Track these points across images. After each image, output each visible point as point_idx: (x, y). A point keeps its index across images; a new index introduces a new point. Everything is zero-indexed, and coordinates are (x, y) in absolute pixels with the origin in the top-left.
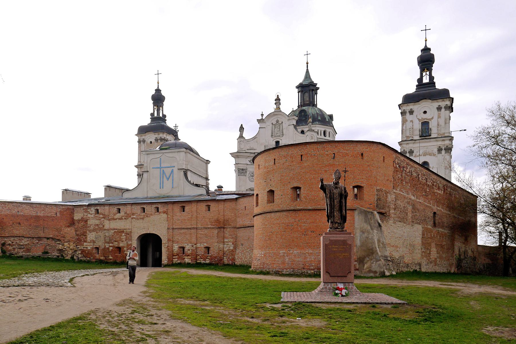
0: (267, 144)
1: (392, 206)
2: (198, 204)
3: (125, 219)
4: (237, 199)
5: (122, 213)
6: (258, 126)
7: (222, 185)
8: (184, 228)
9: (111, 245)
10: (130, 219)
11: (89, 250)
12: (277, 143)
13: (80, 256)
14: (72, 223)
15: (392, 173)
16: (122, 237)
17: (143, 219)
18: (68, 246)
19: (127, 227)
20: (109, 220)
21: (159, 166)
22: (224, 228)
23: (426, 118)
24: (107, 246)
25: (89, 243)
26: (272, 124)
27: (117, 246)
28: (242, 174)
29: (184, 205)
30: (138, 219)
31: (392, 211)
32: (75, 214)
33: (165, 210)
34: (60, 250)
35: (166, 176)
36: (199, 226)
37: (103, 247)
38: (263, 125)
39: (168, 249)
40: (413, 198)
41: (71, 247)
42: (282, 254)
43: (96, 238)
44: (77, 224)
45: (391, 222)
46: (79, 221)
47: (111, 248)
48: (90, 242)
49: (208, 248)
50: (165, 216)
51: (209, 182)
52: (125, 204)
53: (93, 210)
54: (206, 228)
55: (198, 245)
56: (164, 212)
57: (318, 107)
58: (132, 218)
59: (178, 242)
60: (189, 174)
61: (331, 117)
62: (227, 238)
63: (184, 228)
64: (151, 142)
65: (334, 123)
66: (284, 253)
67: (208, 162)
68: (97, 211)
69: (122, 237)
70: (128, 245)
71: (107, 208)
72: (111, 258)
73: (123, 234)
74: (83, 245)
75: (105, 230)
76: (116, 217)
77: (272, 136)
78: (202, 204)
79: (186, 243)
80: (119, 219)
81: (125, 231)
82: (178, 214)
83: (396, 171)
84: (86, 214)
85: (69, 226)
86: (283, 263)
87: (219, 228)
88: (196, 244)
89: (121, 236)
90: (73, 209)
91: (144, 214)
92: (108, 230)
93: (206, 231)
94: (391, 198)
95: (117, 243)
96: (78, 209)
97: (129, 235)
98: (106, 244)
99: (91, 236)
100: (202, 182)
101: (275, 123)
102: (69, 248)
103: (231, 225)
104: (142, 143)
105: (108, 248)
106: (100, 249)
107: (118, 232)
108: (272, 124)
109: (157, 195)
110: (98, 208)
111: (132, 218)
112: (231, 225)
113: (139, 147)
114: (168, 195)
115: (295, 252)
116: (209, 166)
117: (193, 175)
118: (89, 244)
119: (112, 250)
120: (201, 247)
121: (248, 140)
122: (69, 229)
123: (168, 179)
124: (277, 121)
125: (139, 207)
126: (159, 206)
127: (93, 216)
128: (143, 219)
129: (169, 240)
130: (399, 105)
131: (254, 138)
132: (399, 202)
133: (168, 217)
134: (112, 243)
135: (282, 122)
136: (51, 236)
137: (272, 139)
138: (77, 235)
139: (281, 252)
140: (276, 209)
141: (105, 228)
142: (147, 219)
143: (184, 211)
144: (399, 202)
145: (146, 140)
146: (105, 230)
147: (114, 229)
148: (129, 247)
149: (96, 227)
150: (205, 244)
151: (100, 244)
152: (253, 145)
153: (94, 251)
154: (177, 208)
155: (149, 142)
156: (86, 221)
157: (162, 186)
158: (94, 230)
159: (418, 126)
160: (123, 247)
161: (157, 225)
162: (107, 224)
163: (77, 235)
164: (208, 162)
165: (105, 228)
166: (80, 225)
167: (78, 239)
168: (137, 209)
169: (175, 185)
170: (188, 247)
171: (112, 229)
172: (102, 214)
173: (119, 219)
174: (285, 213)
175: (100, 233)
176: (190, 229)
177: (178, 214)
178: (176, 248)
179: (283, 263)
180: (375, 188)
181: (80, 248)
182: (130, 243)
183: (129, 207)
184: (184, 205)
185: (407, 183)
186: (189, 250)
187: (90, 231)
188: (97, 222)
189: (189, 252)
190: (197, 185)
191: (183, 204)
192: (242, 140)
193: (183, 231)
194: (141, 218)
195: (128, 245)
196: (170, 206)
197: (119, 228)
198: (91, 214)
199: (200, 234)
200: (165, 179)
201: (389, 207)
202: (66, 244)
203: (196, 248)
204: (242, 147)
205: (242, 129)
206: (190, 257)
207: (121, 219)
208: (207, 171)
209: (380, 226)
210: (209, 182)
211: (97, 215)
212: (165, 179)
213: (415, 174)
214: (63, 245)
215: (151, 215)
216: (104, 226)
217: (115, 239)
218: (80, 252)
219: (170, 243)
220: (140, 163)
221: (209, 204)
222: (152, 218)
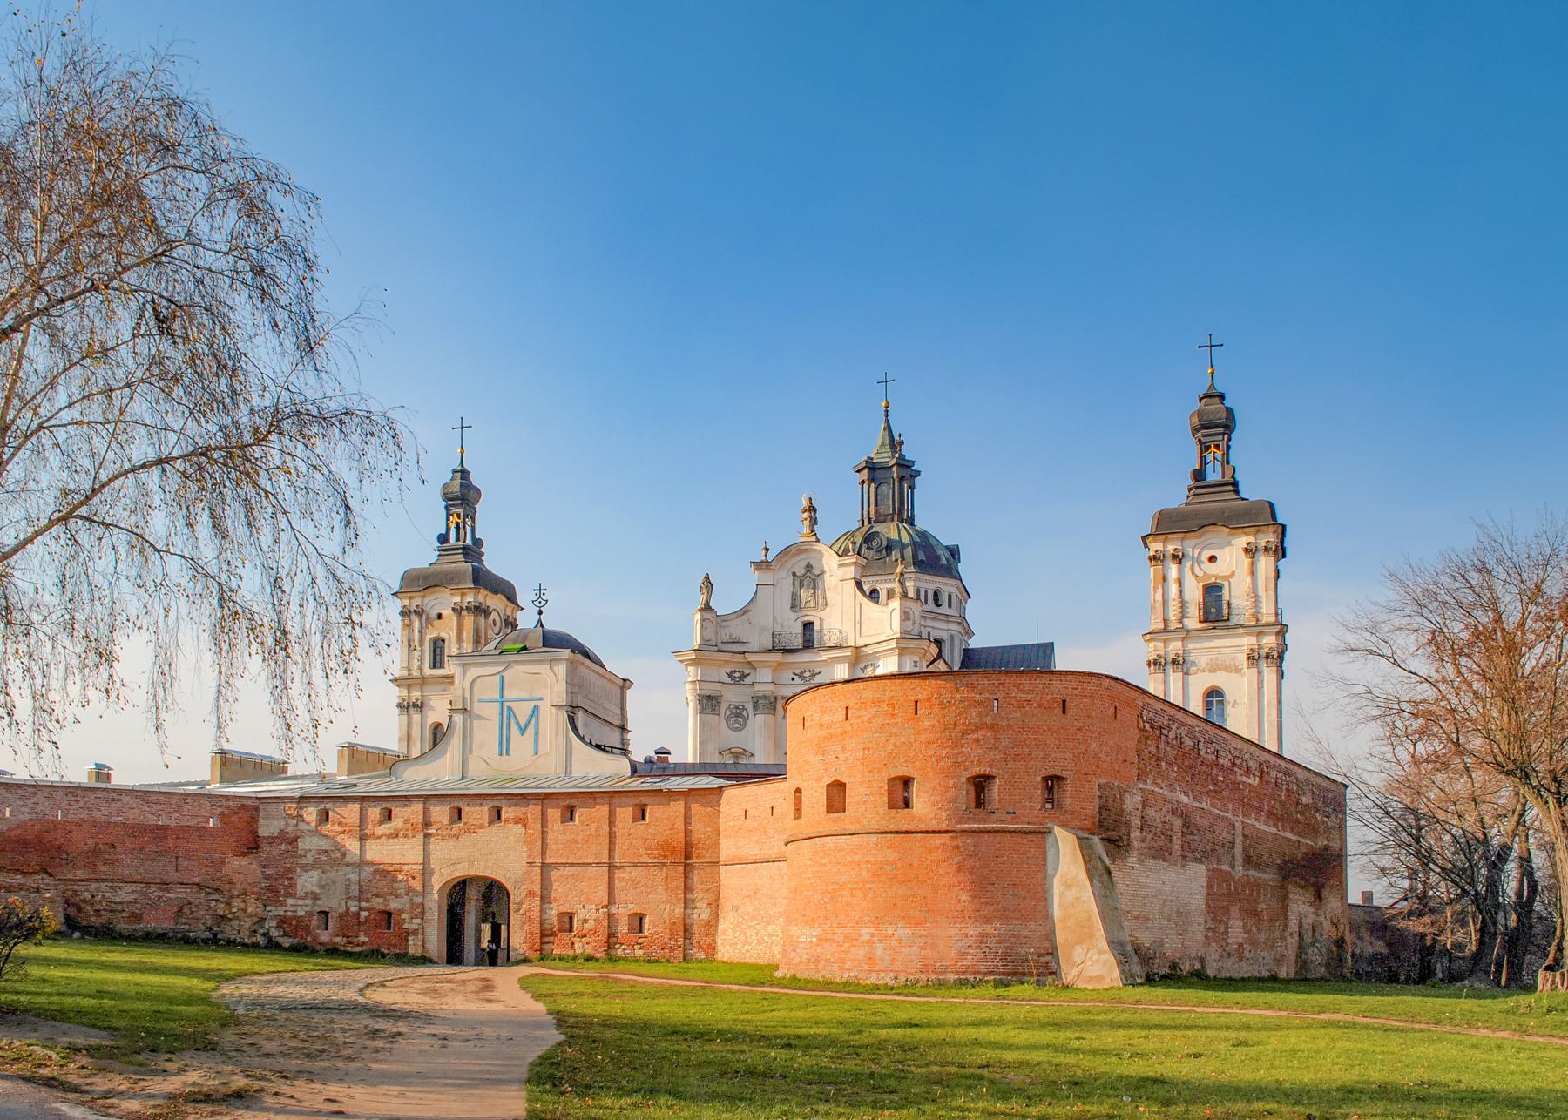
0: (778, 629)
1: (1136, 822)
2: (616, 800)
3: (406, 836)
4: (720, 789)
5: (397, 822)
6: (755, 577)
7: (669, 748)
8: (572, 864)
9: (363, 904)
11: (299, 919)
12: (808, 626)
13: (274, 933)
14: (252, 845)
15: (1133, 744)
17: (457, 837)
21: (497, 696)
24: (353, 909)
26: (794, 574)
29: (573, 802)
31: (1135, 834)
32: (261, 822)
38: (767, 577)
40: (1185, 799)
42: (866, 938)
43: (322, 887)
44: (266, 848)
45: (1133, 859)
46: (272, 840)
47: (364, 914)
50: (519, 829)
51: (629, 736)
52: (407, 799)
54: (635, 865)
55: (614, 910)
56: (517, 821)
57: (920, 524)
60: (581, 717)
61: (954, 552)
63: (572, 864)
65: (962, 568)
66: (872, 935)
67: (626, 683)
70: (414, 906)
74: (283, 904)
75: (348, 865)
77: (793, 607)
78: (623, 800)
80: (390, 836)
81: (405, 868)
83: (1144, 736)
85: (244, 854)
86: (871, 959)
90: (257, 809)
93: (635, 872)
94: (1132, 802)
96: (272, 808)
99: (307, 881)
100: (613, 739)
101: (800, 571)
104: (413, 616)
105: (357, 915)
106: (333, 915)
108: (794, 574)
110: (329, 806)
113: (408, 626)
114: (521, 774)
115: (901, 932)
116: (629, 693)
117: (590, 719)
118: (300, 902)
121: (725, 619)
122: (244, 861)
123: (523, 731)
124: (809, 568)
126: (502, 803)
128: (457, 837)
129: (530, 894)
130: (1144, 538)
131: (744, 611)
132: (1151, 812)
135: (823, 573)
136: (196, 880)
137: (792, 615)
138: (267, 878)
139: (864, 931)
140: (853, 828)
142: (464, 838)
143: (571, 819)
144: (1151, 812)
146: (348, 865)
149: (323, 858)
151: (335, 903)
152: (737, 629)
156: (295, 839)
157: (505, 747)
158: (313, 867)
159: (1194, 593)
160: (400, 912)
161: (499, 852)
163: (267, 878)
164: (626, 683)
166: (275, 852)
167: (270, 889)
168: (440, 813)
173: (390, 836)
174: (873, 838)
175: (332, 874)
179: (871, 959)
180: (1096, 781)
183: (418, 807)
184: (573, 802)
185: (1170, 764)
187: (306, 868)
188: (325, 844)
190: (598, 747)
191: (570, 804)
192: (708, 615)
193: (569, 871)
195: (414, 906)
200: (515, 730)
201: (1128, 825)
204: (710, 634)
205: (708, 585)
208: (623, 708)
209: (1109, 873)
210: (629, 736)
212: (515, 730)
213: (1188, 742)
214: (228, 904)
215: (481, 826)
216: (344, 855)
218: (274, 924)
220: (405, 673)
221: (644, 800)
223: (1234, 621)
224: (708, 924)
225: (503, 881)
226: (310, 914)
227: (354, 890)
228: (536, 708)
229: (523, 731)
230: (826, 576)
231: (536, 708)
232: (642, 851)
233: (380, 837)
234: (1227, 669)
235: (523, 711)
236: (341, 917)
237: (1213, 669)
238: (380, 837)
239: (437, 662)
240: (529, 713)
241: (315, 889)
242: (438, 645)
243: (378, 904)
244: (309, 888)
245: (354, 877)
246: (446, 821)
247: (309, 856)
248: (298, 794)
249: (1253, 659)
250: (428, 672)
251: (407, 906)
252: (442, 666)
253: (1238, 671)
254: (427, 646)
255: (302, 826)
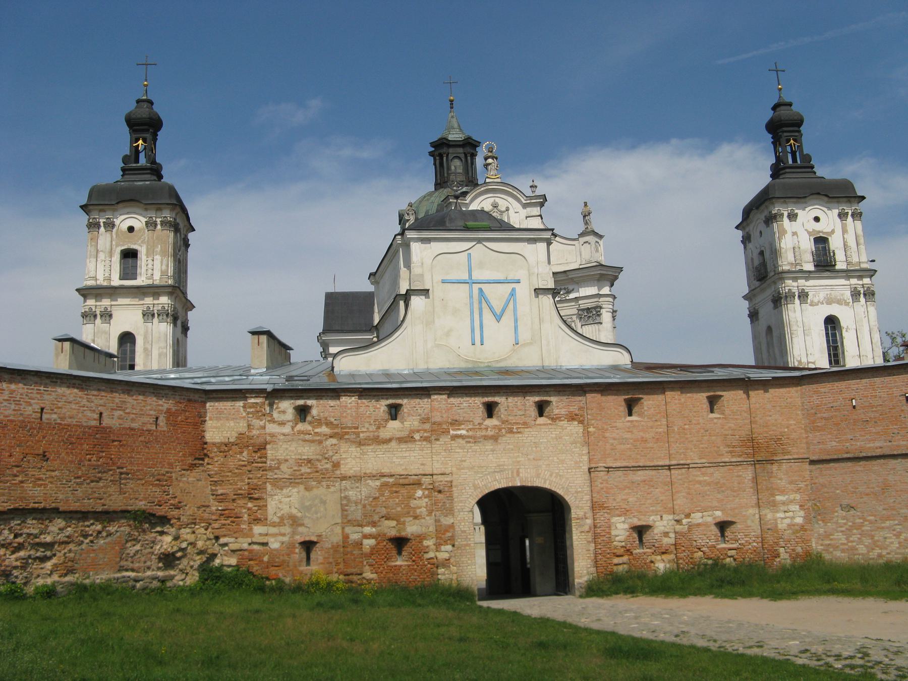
3: (426, 439)
8: (644, 468)
9: (368, 530)
10: (445, 439)
14: (200, 453)
16: (413, 503)
17: (495, 438)
18: (191, 538)
19: (437, 467)
20: (360, 444)
22: (771, 462)
23: (820, 229)
25: (274, 525)
27: (393, 533)
28: (591, 321)
30: (475, 440)
32: (209, 424)
33: (574, 409)
34: (169, 560)
35: (491, 308)
36: (693, 457)
37: (337, 538)
39: (596, 536)
41: (200, 544)
46: (226, 447)
47: (372, 542)
48: (281, 523)
49: (723, 526)
50: (575, 428)
53: (287, 406)
54: (717, 465)
55: (697, 518)
56: (572, 418)
58: (455, 437)
59: (625, 512)
62: (783, 492)
63: (644, 468)
64: (131, 229)
68: (303, 412)
69: (413, 503)
71: (349, 401)
72: (369, 575)
73: (419, 493)
75: (344, 478)
76: (384, 434)
79: (655, 513)
80: (401, 440)
81: (426, 480)
82: (619, 424)
84: (257, 423)
85: (192, 467)
87: (756, 463)
88: (688, 516)
89: (411, 497)
91: (493, 422)
92: (358, 478)
93: (717, 474)
95: (393, 523)
96: (225, 406)
97: (441, 492)
98: (348, 530)
99: (282, 502)
102: (193, 544)
103: (789, 453)
105: (359, 544)
107: (394, 485)
109: (463, 365)
111: (455, 437)
112: (789, 453)
114: (502, 364)
118: (273, 530)
119: (372, 548)
120: (705, 524)
123: (498, 318)
125: (478, 402)
127: (287, 429)
128: (495, 438)
129: (596, 506)
133: (587, 434)
134: (374, 524)
136: (142, 505)
138: (221, 498)
141: (344, 470)
142: (507, 440)
145: (117, 222)
146: (344, 478)
147: (383, 476)
148: (445, 535)
149: (305, 469)
150: (718, 513)
153: (299, 553)
154: (616, 403)
155: (125, 226)
156: (261, 448)
157: (477, 336)
158: (294, 480)
160: (421, 537)
161: (546, 456)
162: (353, 459)
163: (221, 498)
165: (344, 470)
169: (524, 336)
170: (662, 526)
171: (372, 477)
172: (329, 424)
173: (401, 440)
176: (669, 467)
177: (619, 424)
178: (620, 529)
181: (233, 546)
182: (447, 521)
183: (439, 400)
186: (666, 534)
187: (279, 484)
189: (669, 541)
193: (640, 475)
194: (486, 438)
196: (593, 398)
197: (400, 470)
198: (282, 424)
199: (700, 482)
200: (488, 316)
202: (185, 533)
203: (691, 527)
206: (672, 556)
207: (407, 439)
211: (301, 426)
216: (336, 465)
217: (384, 511)
219: (602, 516)
222: (529, 436)
223: (837, 267)
224: (802, 528)
225: (560, 492)
226: (291, 546)
227: (356, 513)
228: (514, 290)
229: (498, 318)
230: (511, 211)
231: (514, 290)
232: (724, 449)
233: (390, 440)
234: (839, 302)
235: (497, 295)
236: (335, 548)
237: (829, 301)
238: (390, 440)
239: (129, 272)
240: (507, 295)
241: (294, 511)
242: (130, 255)
243: (390, 528)
244: (286, 510)
245: (351, 493)
246: (478, 420)
247: (284, 467)
248: (269, 388)
249: (855, 294)
250: (116, 282)
251: (432, 529)
252: (134, 278)
253: (847, 304)
254: (117, 258)
255: (272, 428)
